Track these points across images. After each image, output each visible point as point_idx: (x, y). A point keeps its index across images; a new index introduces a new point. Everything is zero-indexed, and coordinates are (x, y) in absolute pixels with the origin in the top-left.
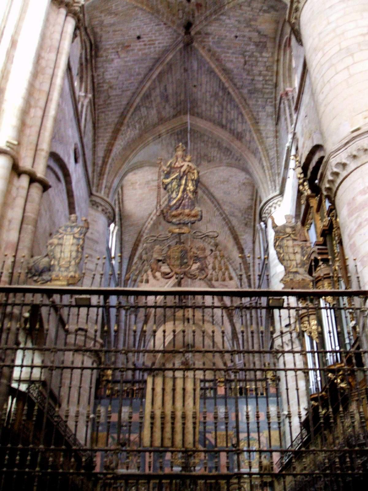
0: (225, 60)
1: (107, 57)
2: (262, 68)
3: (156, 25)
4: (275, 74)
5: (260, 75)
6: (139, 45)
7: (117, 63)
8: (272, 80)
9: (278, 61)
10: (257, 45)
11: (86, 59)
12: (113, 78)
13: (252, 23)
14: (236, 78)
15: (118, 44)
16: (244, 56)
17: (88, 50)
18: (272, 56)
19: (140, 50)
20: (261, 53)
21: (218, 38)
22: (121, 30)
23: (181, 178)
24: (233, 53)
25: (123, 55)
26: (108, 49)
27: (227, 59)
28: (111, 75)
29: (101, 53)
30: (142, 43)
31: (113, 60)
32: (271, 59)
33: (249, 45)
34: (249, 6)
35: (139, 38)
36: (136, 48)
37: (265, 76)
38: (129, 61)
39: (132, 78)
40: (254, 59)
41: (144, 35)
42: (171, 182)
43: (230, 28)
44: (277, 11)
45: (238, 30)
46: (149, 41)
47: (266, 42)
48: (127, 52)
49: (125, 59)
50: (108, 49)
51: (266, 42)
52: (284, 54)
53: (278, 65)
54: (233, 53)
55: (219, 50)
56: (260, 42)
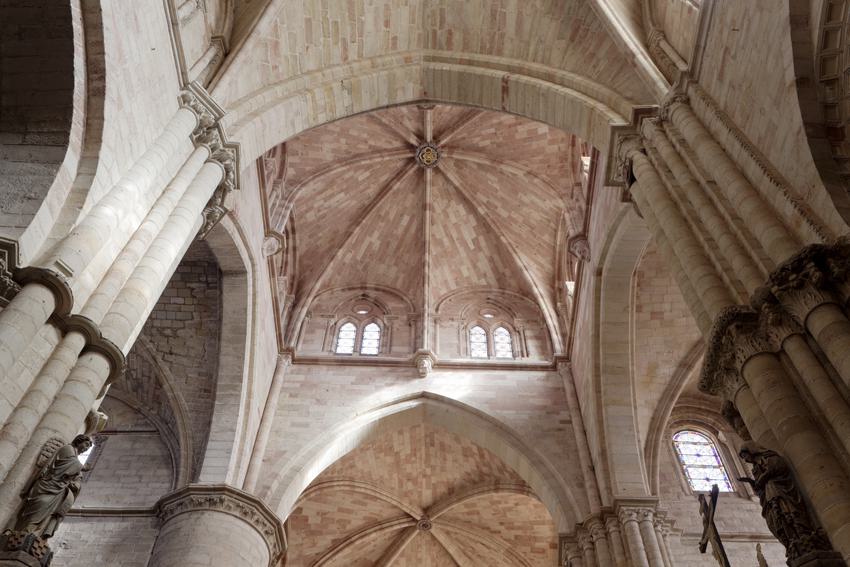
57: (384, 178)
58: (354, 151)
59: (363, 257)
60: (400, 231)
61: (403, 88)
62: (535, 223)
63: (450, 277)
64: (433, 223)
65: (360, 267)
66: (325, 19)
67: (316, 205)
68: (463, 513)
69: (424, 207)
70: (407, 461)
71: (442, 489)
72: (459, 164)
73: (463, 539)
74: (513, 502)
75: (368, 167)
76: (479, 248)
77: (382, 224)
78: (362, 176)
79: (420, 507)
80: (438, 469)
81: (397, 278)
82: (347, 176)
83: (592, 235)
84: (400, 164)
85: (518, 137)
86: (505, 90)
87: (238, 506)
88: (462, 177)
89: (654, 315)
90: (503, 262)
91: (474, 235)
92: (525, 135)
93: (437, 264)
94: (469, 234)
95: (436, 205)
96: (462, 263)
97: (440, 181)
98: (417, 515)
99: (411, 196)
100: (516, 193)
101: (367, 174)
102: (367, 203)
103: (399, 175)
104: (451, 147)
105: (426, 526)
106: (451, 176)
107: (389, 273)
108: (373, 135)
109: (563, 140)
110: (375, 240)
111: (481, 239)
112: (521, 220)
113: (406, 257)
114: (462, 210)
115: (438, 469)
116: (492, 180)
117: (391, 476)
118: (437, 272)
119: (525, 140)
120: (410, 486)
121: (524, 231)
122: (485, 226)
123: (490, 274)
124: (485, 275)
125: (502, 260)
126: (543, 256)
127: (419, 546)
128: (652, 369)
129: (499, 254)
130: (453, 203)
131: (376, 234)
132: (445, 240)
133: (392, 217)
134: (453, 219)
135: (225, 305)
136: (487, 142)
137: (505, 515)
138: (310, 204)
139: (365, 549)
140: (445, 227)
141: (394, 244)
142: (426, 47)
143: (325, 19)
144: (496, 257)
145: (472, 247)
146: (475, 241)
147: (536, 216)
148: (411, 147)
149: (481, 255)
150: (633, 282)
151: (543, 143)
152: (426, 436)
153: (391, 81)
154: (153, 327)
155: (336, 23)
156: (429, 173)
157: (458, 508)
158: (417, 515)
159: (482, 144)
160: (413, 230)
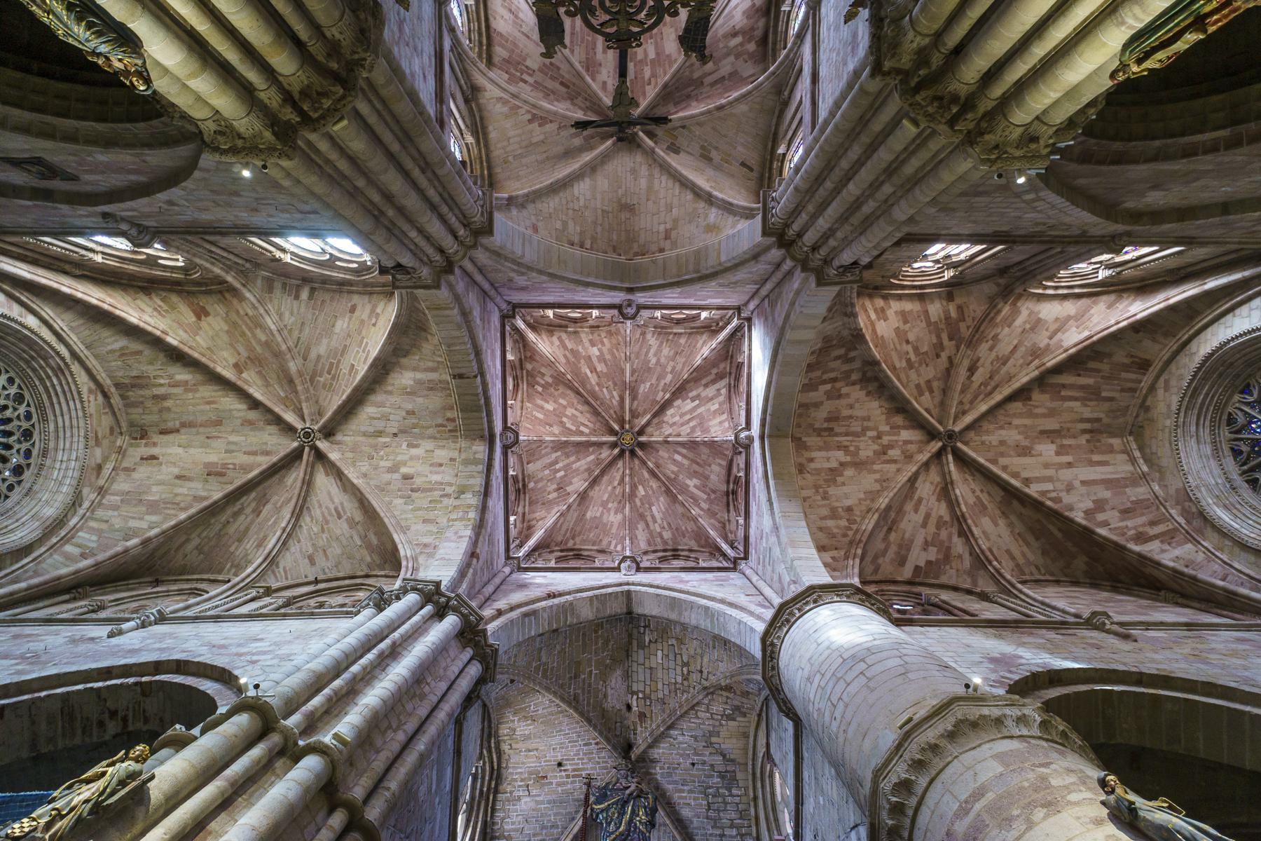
0: (679, 804)
1: (511, 793)
2: (733, 815)
3: (585, 745)
4: (753, 821)
5: (732, 826)
6: (557, 777)
7: (526, 804)
8: (751, 834)
9: (755, 798)
10: (722, 776)
11: (481, 791)
12: (514, 830)
13: (714, 740)
14: (697, 835)
15: (530, 773)
16: (707, 796)
17: (487, 778)
18: (746, 788)
19: (559, 784)
20: (729, 790)
21: (669, 768)
22: (537, 750)
23: (626, 802)
24: (690, 791)
25: (534, 792)
26: (515, 780)
27: (682, 801)
28: (513, 823)
29: (506, 787)
30: (563, 774)
31: (519, 798)
32: (744, 799)
33: (712, 776)
34: (708, 712)
35: (560, 765)
36: (554, 781)
37: (738, 827)
38: (542, 802)
39: (544, 831)
40: (720, 800)
41: (567, 760)
42: (607, 809)
43: (684, 749)
44: (744, 715)
45: (696, 754)
46: (574, 770)
47: (734, 771)
48: (543, 785)
49: (538, 799)
50: (515, 780)
51: (734, 771)
52: (763, 787)
53: (756, 806)
54: (690, 791)
55: (670, 787)
56: (726, 772)
57: (646, 475)
58: (620, 498)
59: (703, 492)
60: (686, 462)
61: (475, 453)
62: (672, 352)
63: (718, 420)
64: (679, 435)
65: (713, 496)
66: (426, 509)
67: (658, 530)
68: (933, 398)
69: (667, 442)
70: (856, 454)
71: (899, 420)
72: (635, 415)
73: (969, 397)
74: (904, 345)
75: (634, 487)
76: (698, 397)
77: (681, 477)
78: (641, 491)
79: (928, 442)
80: (865, 424)
81: (720, 465)
82: (638, 503)
83: (617, 301)
84: (637, 462)
85: (605, 370)
86: (461, 376)
87: (780, 627)
88: (645, 412)
89: (667, 237)
90: (707, 376)
91: (689, 401)
92: (603, 365)
93: (706, 430)
94: (689, 405)
95: (667, 433)
96: (709, 410)
97: (649, 430)
98: (936, 445)
99: (661, 453)
100: (650, 368)
101: (640, 488)
102: (663, 489)
103: (644, 463)
104: (622, 422)
105: (951, 435)
106: (644, 421)
107: (716, 472)
108: (610, 482)
109: (599, 335)
110: (692, 483)
111: (694, 393)
112: (671, 363)
113: (704, 457)
114: (670, 412)
115: (865, 424)
116: (643, 388)
117: (875, 472)
118: (712, 430)
119: (606, 365)
120: (894, 453)
121: (681, 360)
122: (680, 391)
123: (717, 386)
124: (718, 390)
125: (700, 375)
126: (697, 342)
127: (983, 443)
128: (711, 228)
129: (701, 379)
130: (665, 419)
131: (688, 482)
132: (691, 424)
133: (676, 469)
134: (677, 418)
135: (654, 613)
136: (615, 393)
137: (926, 353)
138: (655, 534)
139: (986, 503)
140: (682, 425)
141: (695, 467)
142: (457, 437)
143: (426, 509)
144: (704, 382)
145: (697, 402)
146: (693, 400)
147: (666, 351)
148: (622, 452)
149: (703, 394)
150: (638, 260)
151: (605, 350)
152: (819, 435)
153: (466, 462)
154: (682, 684)
155: (431, 501)
156: (642, 439)
157: (923, 405)
158: (936, 445)
159: (617, 398)
160: (684, 451)
